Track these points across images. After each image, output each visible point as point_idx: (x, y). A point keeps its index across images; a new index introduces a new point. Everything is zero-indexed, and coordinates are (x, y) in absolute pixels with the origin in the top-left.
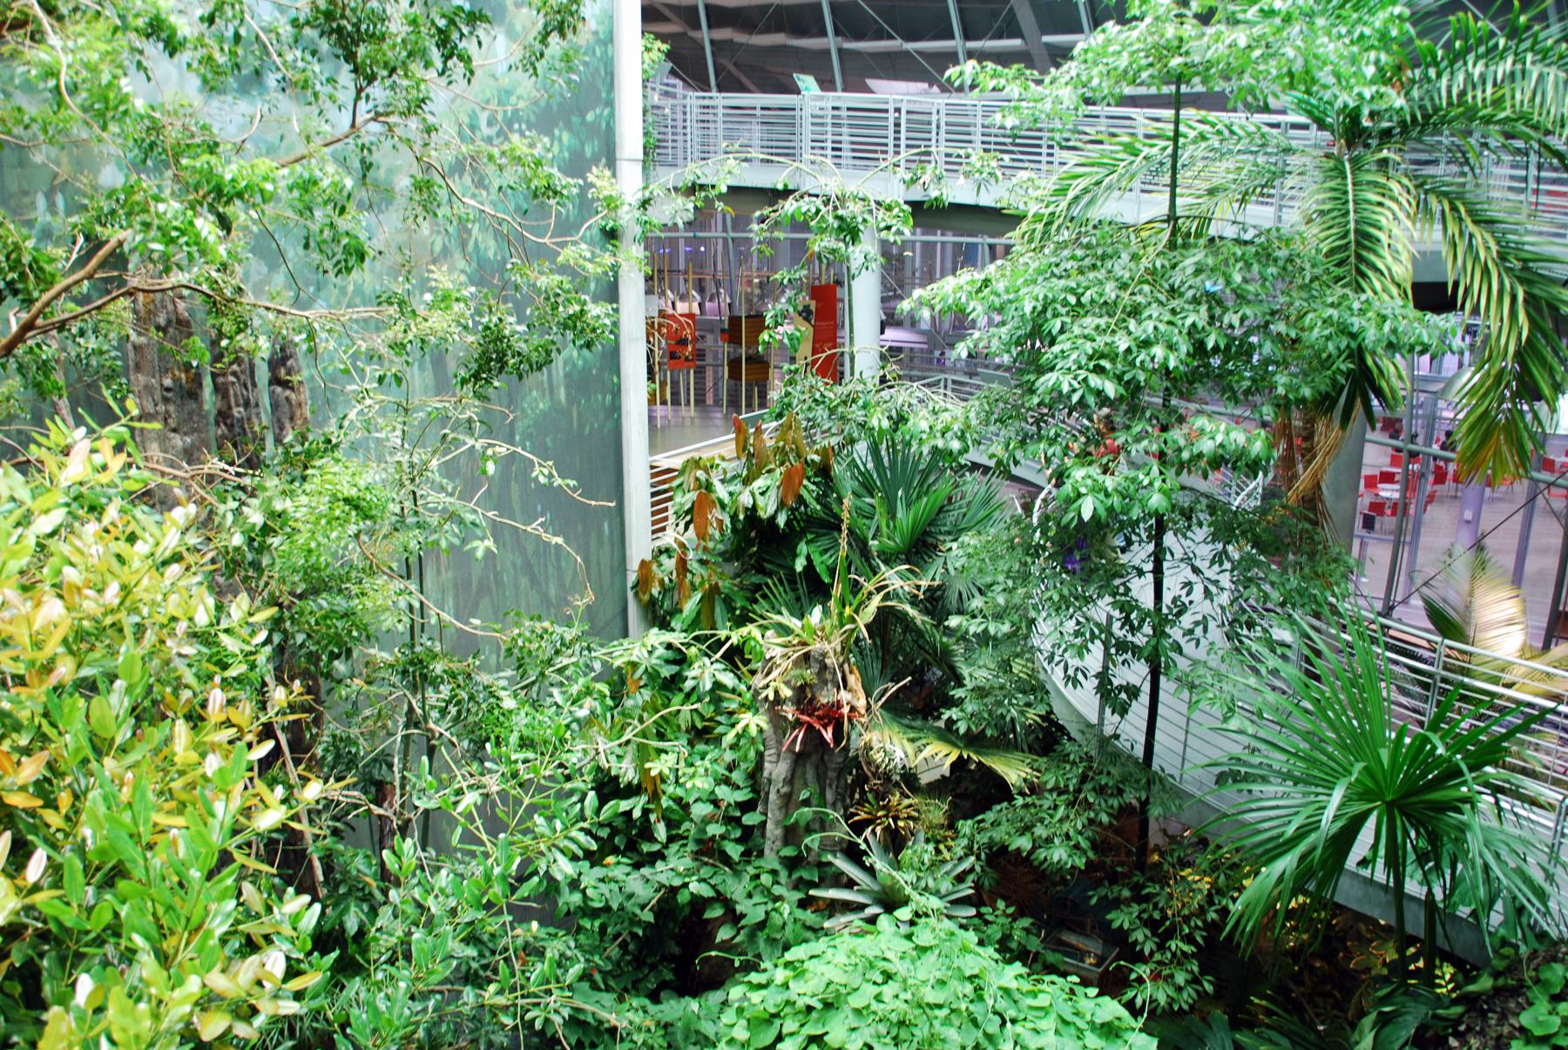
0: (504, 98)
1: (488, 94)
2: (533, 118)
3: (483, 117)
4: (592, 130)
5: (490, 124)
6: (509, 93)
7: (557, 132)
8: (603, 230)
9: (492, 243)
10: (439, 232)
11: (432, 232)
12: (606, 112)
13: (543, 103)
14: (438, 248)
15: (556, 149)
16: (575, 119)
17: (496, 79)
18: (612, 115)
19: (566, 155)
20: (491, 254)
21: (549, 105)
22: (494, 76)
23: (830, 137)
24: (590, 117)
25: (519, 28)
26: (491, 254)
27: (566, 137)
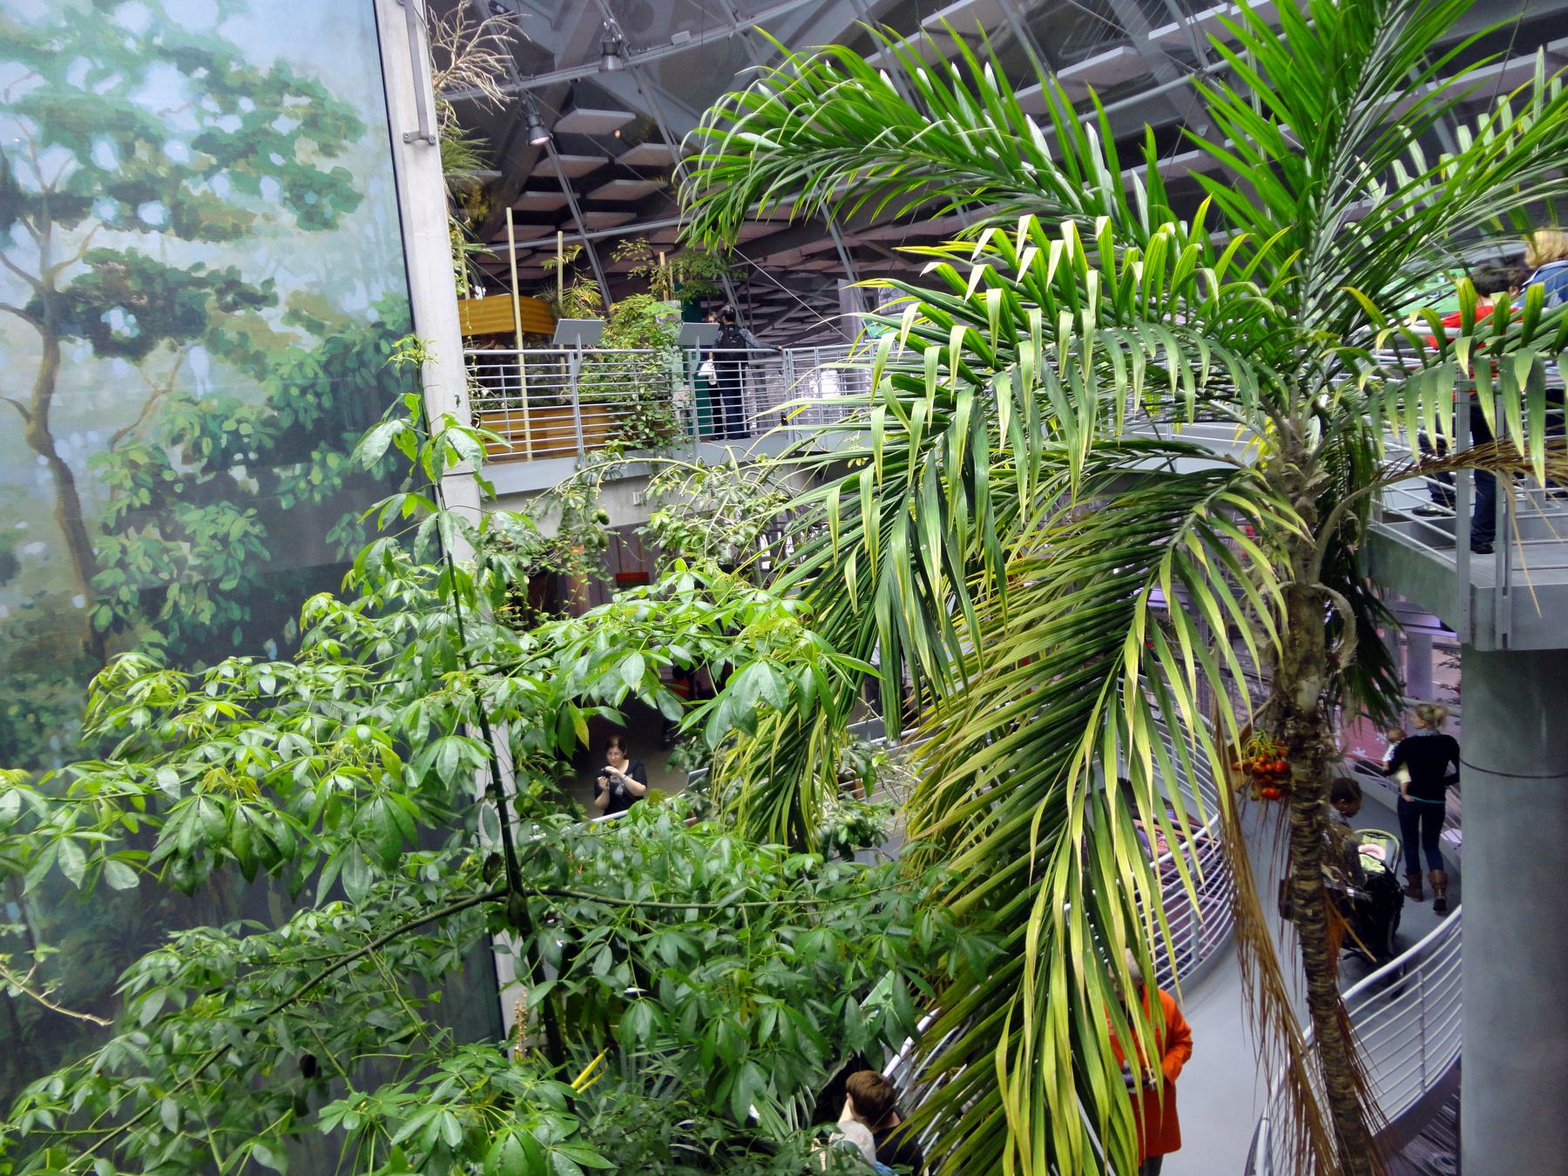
0: (212, 426)
1: (181, 422)
2: (269, 444)
3: (176, 454)
5: (187, 459)
6: (221, 418)
7: (316, 455)
10: (104, 602)
11: (91, 603)
13: (286, 422)
14: (104, 617)
15: (316, 476)
17: (196, 404)
19: (337, 481)
20: (205, 618)
21: (297, 426)
22: (189, 400)
23: (724, 416)
25: (231, 335)
26: (205, 618)
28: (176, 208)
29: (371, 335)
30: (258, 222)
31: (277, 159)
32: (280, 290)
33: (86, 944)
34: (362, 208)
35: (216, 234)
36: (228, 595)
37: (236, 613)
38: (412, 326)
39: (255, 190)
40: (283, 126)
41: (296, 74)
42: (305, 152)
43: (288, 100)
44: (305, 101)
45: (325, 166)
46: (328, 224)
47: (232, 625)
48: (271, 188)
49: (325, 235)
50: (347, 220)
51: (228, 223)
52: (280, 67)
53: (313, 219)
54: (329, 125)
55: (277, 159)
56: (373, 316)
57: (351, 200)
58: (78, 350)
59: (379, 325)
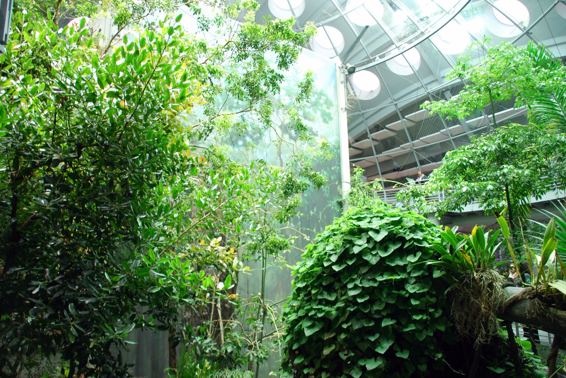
4: (333, 172)
8: (337, 202)
9: (301, 198)
12: (338, 168)
13: (318, 162)
16: (328, 168)
18: (340, 169)
24: (333, 168)
27: (325, 173)
28: (304, 113)
29: (333, 147)
30: (316, 119)
31: (320, 108)
32: (319, 134)
33: (273, 274)
34: (333, 120)
35: (310, 120)
36: (305, 197)
37: (306, 202)
38: (339, 148)
39: (316, 113)
40: (322, 101)
41: (324, 92)
42: (324, 107)
43: (323, 97)
44: (325, 98)
45: (327, 111)
46: (327, 123)
47: (305, 205)
48: (319, 113)
49: (326, 124)
50: (330, 122)
51: (312, 118)
52: (322, 91)
53: (325, 121)
54: (328, 103)
55: (320, 108)
56: (333, 144)
57: (331, 119)
58: (286, 137)
59: (334, 146)
